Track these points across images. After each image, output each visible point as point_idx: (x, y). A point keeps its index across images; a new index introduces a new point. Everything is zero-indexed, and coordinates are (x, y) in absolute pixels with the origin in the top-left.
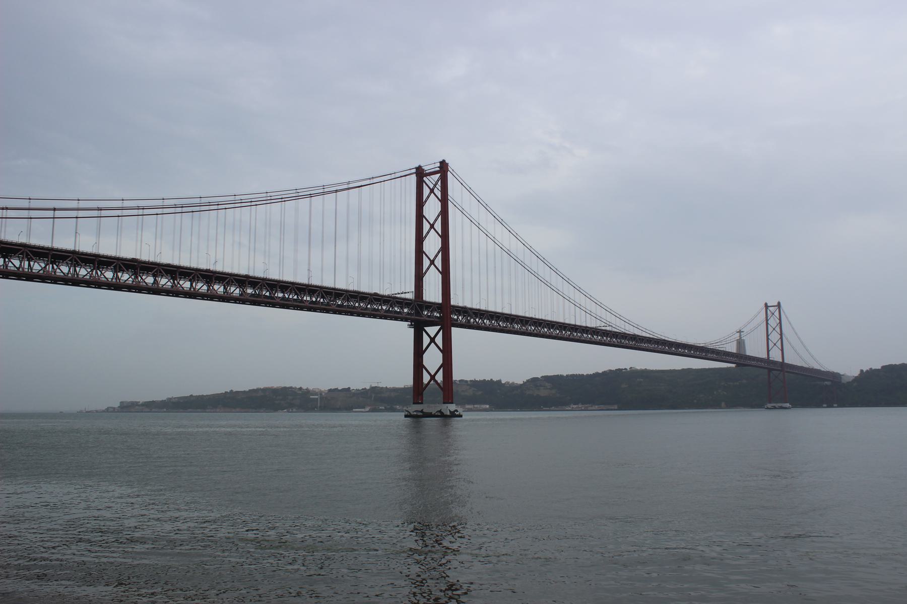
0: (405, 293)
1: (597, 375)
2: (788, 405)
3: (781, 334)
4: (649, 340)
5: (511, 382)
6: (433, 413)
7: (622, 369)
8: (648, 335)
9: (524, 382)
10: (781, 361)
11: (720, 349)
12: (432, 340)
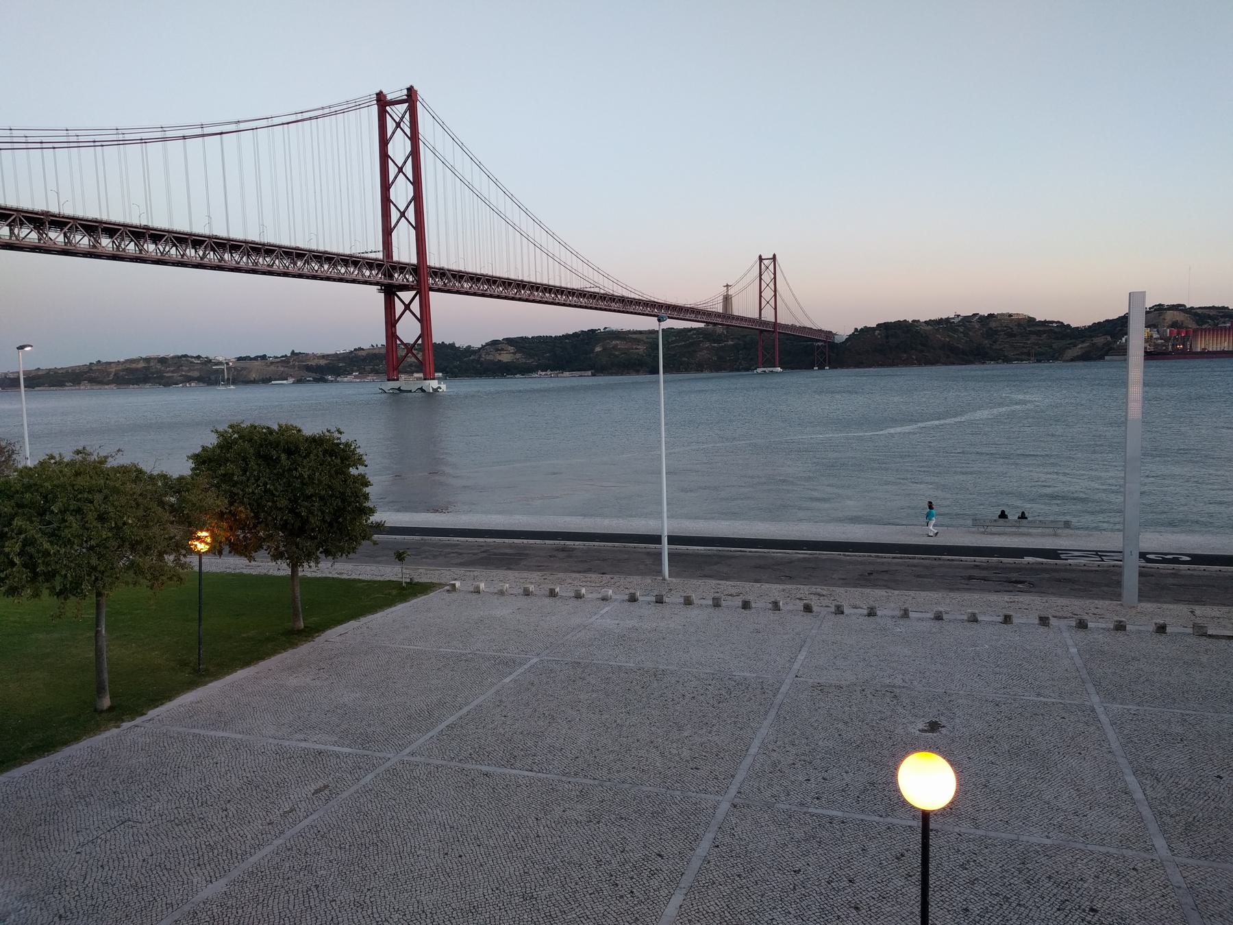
0: (375, 252)
1: (567, 336)
3: (775, 291)
4: (638, 302)
8: (637, 297)
10: (774, 321)
11: (711, 310)
12: (407, 307)
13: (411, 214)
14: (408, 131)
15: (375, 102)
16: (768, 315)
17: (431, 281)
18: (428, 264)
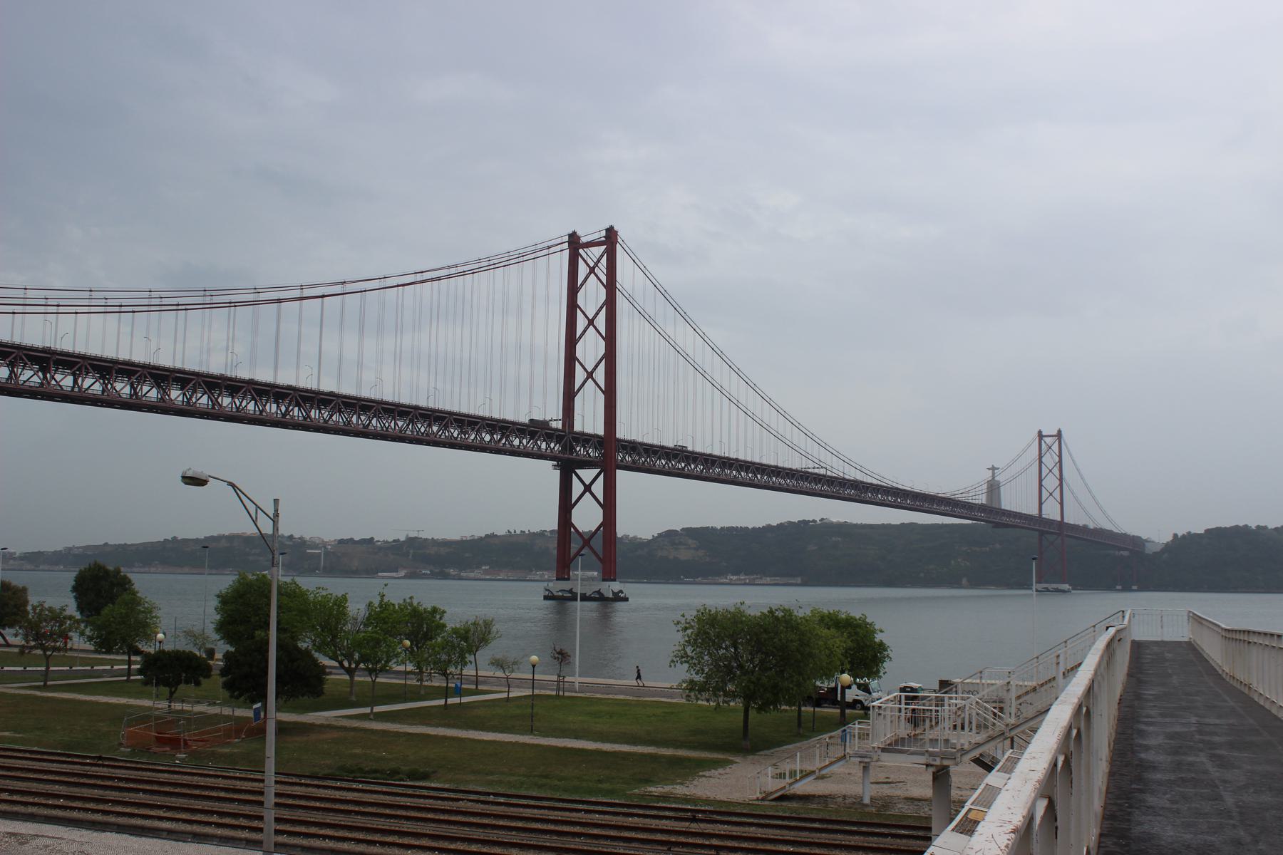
1: (768, 528)
2: (1066, 587)
3: (1061, 479)
4: (876, 489)
5: (631, 536)
6: (587, 595)
8: (875, 482)
9: (653, 536)
10: (1059, 519)
11: (974, 502)
12: (588, 488)
13: (600, 375)
14: (604, 279)
15: (566, 245)
16: (1051, 512)
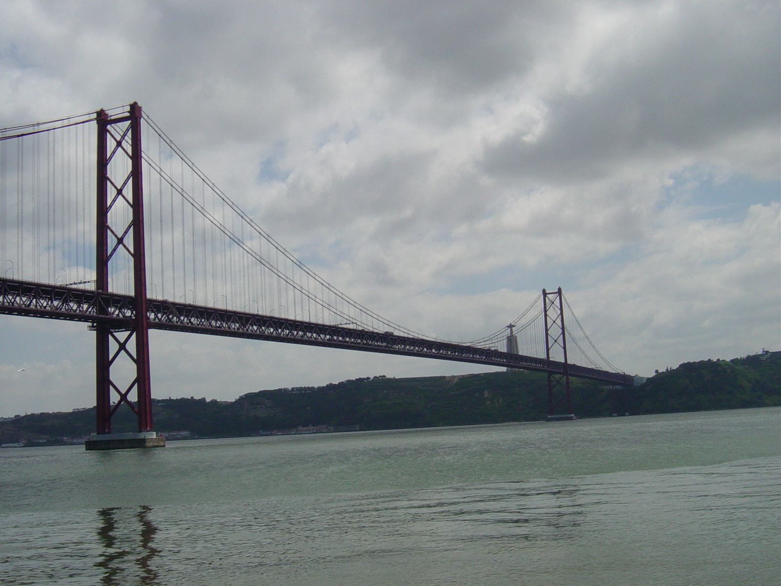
0: (85, 282)
1: (331, 387)
3: (563, 328)
7: (364, 379)
12: (122, 346)
17: (152, 316)
18: (149, 296)
